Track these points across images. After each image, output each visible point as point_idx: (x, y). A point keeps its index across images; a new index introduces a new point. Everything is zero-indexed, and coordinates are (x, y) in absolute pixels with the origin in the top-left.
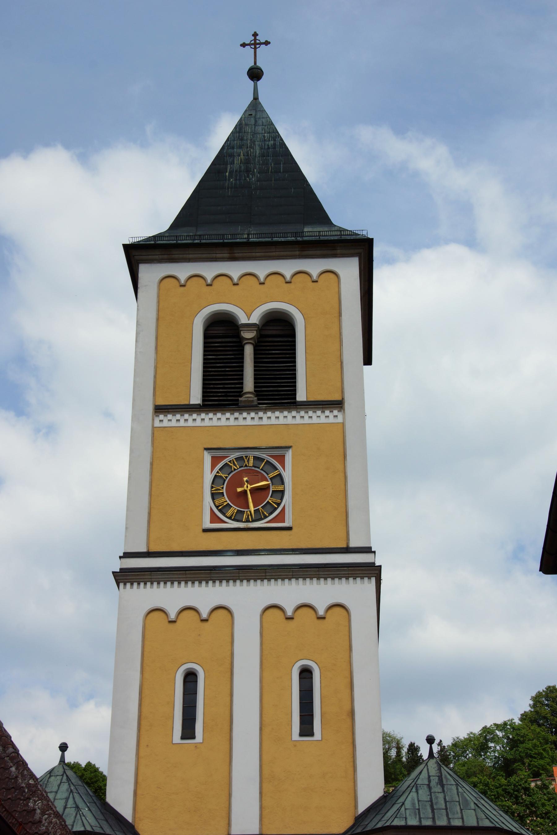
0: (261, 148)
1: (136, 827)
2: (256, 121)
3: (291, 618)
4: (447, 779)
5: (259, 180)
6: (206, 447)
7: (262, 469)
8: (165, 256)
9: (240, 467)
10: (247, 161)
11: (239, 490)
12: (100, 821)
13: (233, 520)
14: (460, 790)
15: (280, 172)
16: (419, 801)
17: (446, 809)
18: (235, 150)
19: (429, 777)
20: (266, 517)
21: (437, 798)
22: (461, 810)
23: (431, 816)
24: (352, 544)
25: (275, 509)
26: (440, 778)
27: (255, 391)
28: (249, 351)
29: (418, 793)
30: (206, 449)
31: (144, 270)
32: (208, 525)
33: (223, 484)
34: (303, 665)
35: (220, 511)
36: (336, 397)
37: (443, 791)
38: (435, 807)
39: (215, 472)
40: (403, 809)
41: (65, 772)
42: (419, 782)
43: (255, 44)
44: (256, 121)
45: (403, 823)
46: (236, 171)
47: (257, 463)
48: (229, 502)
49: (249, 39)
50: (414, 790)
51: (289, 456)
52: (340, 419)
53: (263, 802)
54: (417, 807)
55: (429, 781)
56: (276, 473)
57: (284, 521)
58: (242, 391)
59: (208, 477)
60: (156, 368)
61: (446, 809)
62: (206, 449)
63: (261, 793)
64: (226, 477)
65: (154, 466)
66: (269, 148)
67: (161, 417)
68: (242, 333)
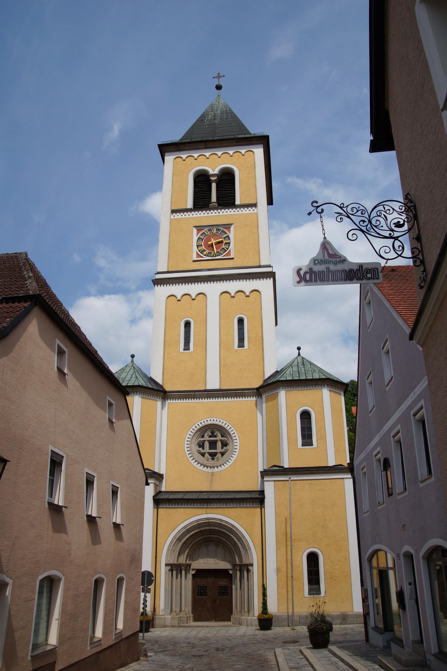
0: (221, 111)
1: (164, 386)
2: (219, 103)
3: (234, 297)
4: (306, 363)
5: (219, 122)
6: (194, 226)
7: (220, 234)
8: (177, 149)
9: (210, 234)
10: (215, 116)
11: (209, 243)
12: (147, 383)
13: (207, 256)
14: (312, 366)
15: (229, 118)
16: (292, 371)
17: (305, 373)
18: (209, 113)
19: (298, 362)
20: (222, 254)
21: (301, 370)
22: (312, 373)
23: (298, 376)
24: (262, 264)
25: (226, 251)
27: (217, 201)
28: (214, 185)
29: (292, 369)
30: (194, 227)
32: (195, 258)
33: (202, 241)
34: (239, 317)
35: (201, 253)
36: (253, 202)
37: (304, 367)
38: (300, 373)
39: (198, 236)
40: (285, 374)
41: (133, 365)
42: (293, 364)
43: (219, 77)
44: (219, 103)
45: (285, 379)
46: (209, 119)
47: (218, 231)
48: (205, 248)
49: (216, 75)
50: (291, 367)
51: (232, 228)
53: (221, 375)
54: (292, 373)
55: (298, 364)
56: (226, 235)
57: (230, 256)
58: (211, 202)
59: (195, 238)
60: (172, 194)
61: (305, 373)
62: (194, 227)
63: (220, 372)
64: (204, 238)
65: (171, 235)
66: (224, 111)
67: (174, 214)
68: (211, 178)
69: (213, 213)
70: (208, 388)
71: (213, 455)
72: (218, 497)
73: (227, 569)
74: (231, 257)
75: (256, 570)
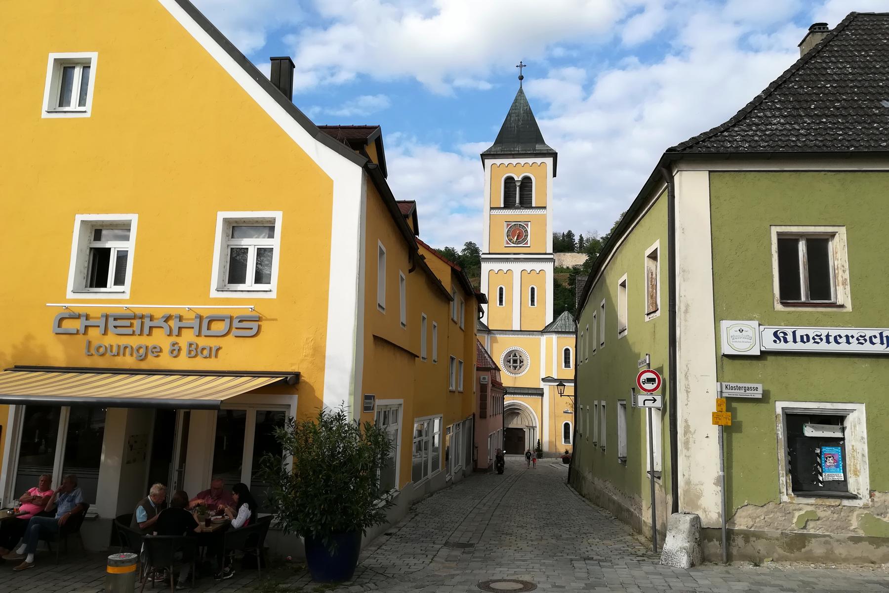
5: (522, 124)
26: (568, 317)
28: (518, 189)
31: (486, 161)
49: (519, 64)
51: (529, 223)
52: (545, 213)
67: (492, 211)
69: (517, 212)
70: (513, 329)
71: (515, 367)
72: (519, 391)
73: (522, 429)
74: (529, 245)
75: (538, 430)
